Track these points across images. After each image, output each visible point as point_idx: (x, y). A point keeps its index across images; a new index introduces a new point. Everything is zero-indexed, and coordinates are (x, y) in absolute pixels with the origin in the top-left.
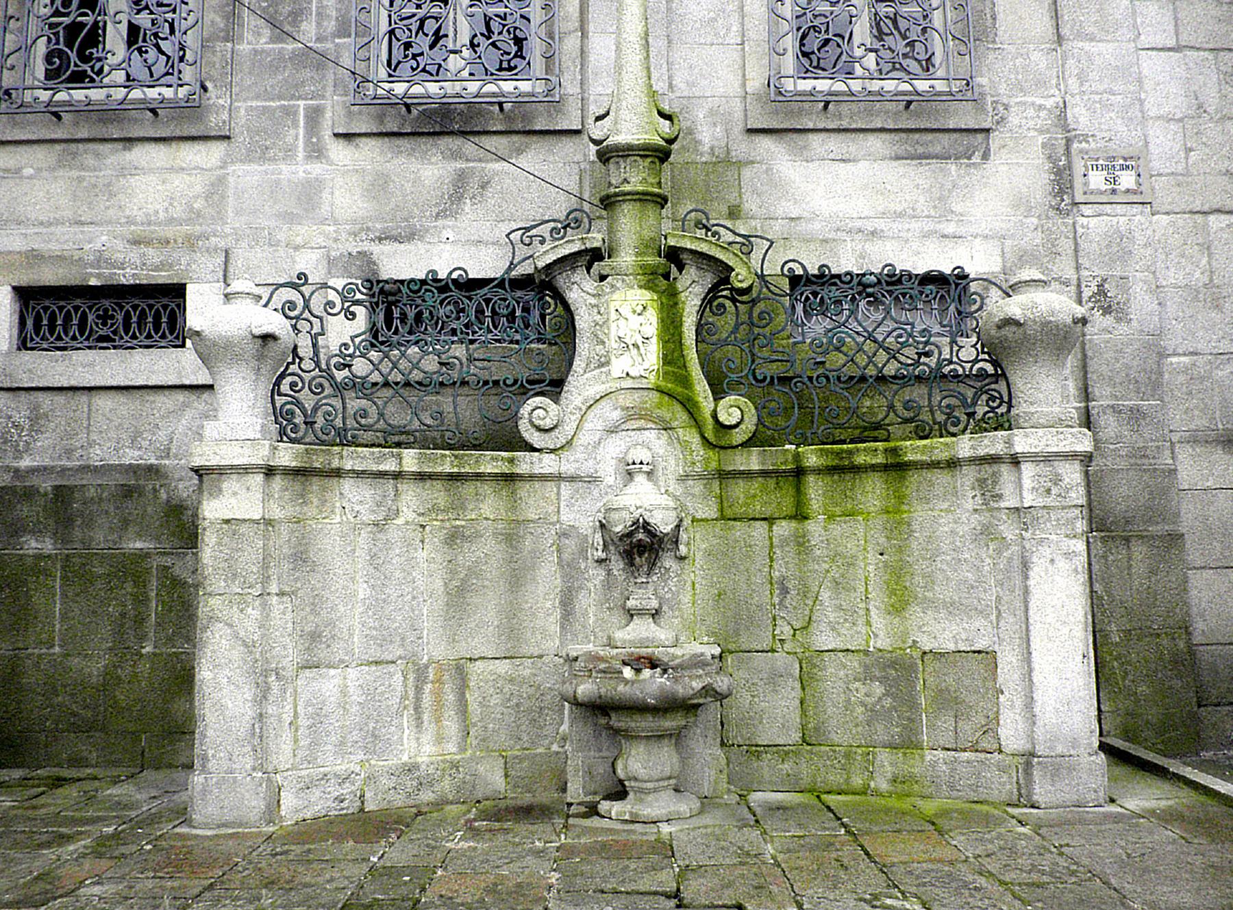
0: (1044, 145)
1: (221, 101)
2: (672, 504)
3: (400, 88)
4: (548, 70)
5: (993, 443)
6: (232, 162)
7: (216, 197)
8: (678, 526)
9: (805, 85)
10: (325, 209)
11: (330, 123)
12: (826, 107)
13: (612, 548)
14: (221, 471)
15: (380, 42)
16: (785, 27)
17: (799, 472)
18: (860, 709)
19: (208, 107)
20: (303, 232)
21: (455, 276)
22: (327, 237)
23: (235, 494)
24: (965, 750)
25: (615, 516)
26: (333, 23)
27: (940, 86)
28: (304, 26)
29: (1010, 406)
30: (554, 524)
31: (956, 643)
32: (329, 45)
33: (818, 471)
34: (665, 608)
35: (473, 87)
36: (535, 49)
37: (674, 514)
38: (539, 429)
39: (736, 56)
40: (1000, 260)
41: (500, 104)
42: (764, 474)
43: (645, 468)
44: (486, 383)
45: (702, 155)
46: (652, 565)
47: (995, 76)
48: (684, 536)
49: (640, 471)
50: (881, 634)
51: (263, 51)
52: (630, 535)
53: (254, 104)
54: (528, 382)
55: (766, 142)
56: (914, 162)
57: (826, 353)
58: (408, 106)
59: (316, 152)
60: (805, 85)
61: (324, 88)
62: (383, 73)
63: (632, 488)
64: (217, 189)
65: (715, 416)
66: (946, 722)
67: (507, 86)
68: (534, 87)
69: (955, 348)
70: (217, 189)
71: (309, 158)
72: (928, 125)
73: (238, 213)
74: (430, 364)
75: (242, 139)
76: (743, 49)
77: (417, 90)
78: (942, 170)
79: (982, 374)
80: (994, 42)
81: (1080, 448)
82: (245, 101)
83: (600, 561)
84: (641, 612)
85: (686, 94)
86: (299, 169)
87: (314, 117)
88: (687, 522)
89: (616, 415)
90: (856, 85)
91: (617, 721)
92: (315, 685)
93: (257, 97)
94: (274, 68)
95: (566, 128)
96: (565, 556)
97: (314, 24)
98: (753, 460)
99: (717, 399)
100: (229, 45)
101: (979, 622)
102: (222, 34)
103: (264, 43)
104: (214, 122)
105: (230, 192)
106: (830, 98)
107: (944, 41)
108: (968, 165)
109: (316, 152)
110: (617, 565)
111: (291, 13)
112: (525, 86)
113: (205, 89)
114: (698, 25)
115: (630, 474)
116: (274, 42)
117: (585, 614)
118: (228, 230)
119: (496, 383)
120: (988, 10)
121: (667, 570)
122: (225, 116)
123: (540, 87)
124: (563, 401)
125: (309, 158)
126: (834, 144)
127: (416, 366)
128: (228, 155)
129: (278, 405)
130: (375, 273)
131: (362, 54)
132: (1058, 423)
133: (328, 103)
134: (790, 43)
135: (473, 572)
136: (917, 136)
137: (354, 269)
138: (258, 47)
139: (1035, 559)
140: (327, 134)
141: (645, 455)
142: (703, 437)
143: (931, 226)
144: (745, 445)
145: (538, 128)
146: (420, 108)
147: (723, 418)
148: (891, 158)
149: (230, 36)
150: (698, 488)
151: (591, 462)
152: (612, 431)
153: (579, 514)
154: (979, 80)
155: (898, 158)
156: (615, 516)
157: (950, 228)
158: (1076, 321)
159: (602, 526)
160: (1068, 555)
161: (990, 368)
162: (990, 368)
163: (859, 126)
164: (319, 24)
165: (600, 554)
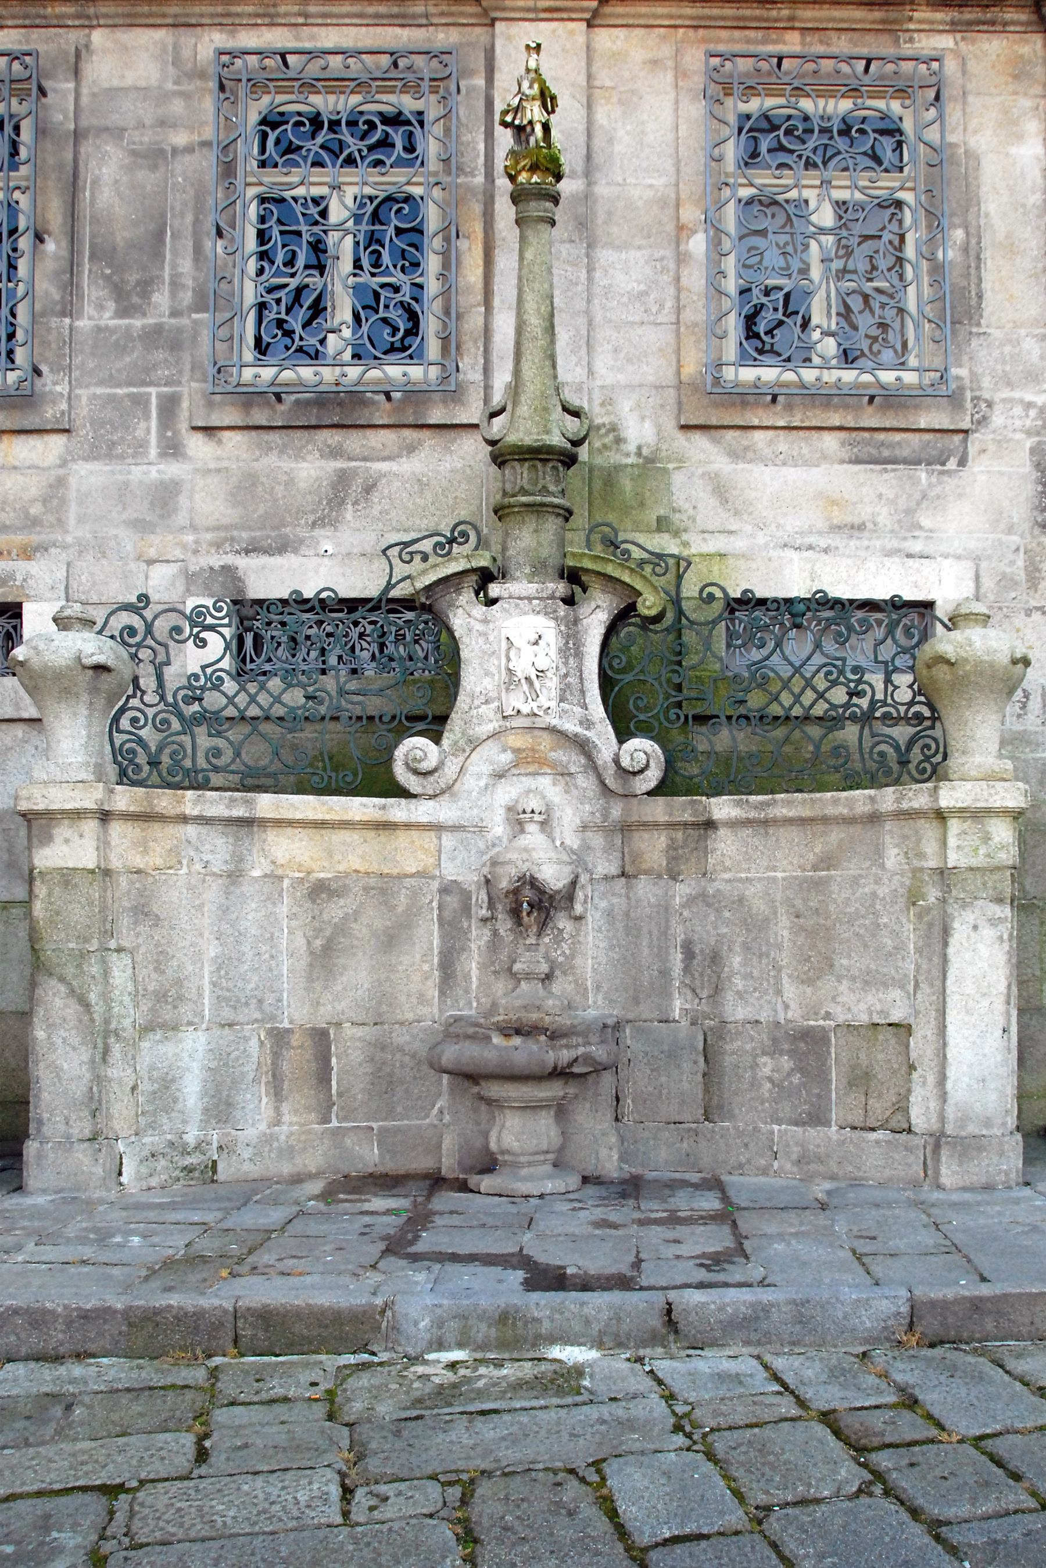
0: (1032, 451)
1: (58, 388)
2: (565, 858)
3: (267, 373)
4: (445, 349)
5: (917, 797)
6: (73, 460)
7: (55, 502)
8: (574, 883)
9: (748, 374)
10: (182, 518)
11: (186, 414)
12: (774, 399)
13: (500, 907)
14: (50, 817)
15: (243, 320)
16: (726, 304)
17: (710, 825)
18: (768, 1085)
19: (44, 395)
20: (155, 544)
21: (324, 595)
22: (184, 547)
23: (67, 841)
24: (873, 1129)
25: (500, 870)
26: (190, 294)
27: (909, 378)
28: (156, 297)
29: (945, 757)
30: (433, 878)
31: (871, 1015)
32: (185, 321)
33: (735, 824)
34: (557, 973)
35: (354, 372)
36: (430, 325)
37: (568, 869)
38: (416, 772)
39: (671, 338)
40: (972, 585)
41: (388, 395)
42: (672, 826)
43: (537, 818)
44: (359, 718)
45: (628, 455)
46: (542, 926)
47: (980, 365)
48: (580, 895)
49: (532, 820)
50: (793, 1005)
51: (107, 327)
52: (516, 892)
53: (100, 391)
54: (409, 718)
55: (700, 442)
56: (879, 467)
57: (747, 690)
58: (278, 397)
59: (172, 449)
60: (748, 374)
61: (180, 372)
62: (249, 355)
63: (524, 841)
64: (56, 492)
65: (617, 761)
66: (855, 1099)
67: (394, 372)
68: (426, 373)
69: (890, 688)
70: (56, 492)
71: (163, 455)
72: (895, 424)
73: (81, 520)
74: (295, 697)
75: (85, 431)
76: (678, 330)
77: (287, 375)
78: (910, 478)
79: (919, 717)
80: (979, 325)
81: (1011, 804)
82: (87, 386)
83: (484, 920)
84: (528, 976)
85: (609, 381)
86: (154, 470)
87: (169, 407)
88: (584, 879)
89: (507, 757)
90: (809, 375)
91: (494, 1090)
92: (162, 1049)
93: (101, 383)
94: (121, 349)
95: (465, 421)
96: (446, 914)
97: (167, 293)
98: (659, 809)
99: (621, 741)
100: (67, 321)
101: (896, 994)
102: (58, 308)
103: (108, 318)
104: (50, 413)
105: (72, 495)
106: (776, 390)
107: (917, 326)
108: (942, 473)
109: (172, 449)
110: (504, 925)
111: (138, 283)
112: (416, 372)
113: (37, 372)
114: (625, 299)
115: (520, 823)
116: (121, 317)
117: (467, 977)
118: (69, 539)
119: (371, 718)
120: (973, 287)
121: (561, 931)
122: (64, 406)
123: (434, 372)
124: (446, 742)
125: (163, 455)
126: (784, 443)
127: (277, 700)
128: (69, 452)
129: (117, 743)
130: (241, 591)
131: (223, 333)
132: (991, 777)
133: (185, 390)
134: (733, 325)
135: (341, 929)
136: (882, 436)
137: (217, 587)
138: (102, 323)
139: (956, 925)
140: (183, 426)
141: (534, 803)
142: (602, 783)
143: (895, 544)
144: (649, 793)
145: (431, 422)
146: (293, 397)
147: (625, 762)
148: (851, 462)
149: (68, 309)
150: (597, 840)
151: (475, 811)
152: (499, 775)
153: (460, 866)
154: (954, 371)
155: (858, 461)
156: (500, 870)
157: (917, 547)
158: (1014, 662)
159: (488, 881)
160: (994, 922)
161: (927, 713)
162: (927, 713)
163: (814, 423)
164: (173, 295)
165: (484, 912)
